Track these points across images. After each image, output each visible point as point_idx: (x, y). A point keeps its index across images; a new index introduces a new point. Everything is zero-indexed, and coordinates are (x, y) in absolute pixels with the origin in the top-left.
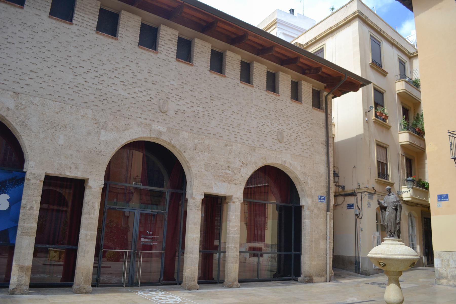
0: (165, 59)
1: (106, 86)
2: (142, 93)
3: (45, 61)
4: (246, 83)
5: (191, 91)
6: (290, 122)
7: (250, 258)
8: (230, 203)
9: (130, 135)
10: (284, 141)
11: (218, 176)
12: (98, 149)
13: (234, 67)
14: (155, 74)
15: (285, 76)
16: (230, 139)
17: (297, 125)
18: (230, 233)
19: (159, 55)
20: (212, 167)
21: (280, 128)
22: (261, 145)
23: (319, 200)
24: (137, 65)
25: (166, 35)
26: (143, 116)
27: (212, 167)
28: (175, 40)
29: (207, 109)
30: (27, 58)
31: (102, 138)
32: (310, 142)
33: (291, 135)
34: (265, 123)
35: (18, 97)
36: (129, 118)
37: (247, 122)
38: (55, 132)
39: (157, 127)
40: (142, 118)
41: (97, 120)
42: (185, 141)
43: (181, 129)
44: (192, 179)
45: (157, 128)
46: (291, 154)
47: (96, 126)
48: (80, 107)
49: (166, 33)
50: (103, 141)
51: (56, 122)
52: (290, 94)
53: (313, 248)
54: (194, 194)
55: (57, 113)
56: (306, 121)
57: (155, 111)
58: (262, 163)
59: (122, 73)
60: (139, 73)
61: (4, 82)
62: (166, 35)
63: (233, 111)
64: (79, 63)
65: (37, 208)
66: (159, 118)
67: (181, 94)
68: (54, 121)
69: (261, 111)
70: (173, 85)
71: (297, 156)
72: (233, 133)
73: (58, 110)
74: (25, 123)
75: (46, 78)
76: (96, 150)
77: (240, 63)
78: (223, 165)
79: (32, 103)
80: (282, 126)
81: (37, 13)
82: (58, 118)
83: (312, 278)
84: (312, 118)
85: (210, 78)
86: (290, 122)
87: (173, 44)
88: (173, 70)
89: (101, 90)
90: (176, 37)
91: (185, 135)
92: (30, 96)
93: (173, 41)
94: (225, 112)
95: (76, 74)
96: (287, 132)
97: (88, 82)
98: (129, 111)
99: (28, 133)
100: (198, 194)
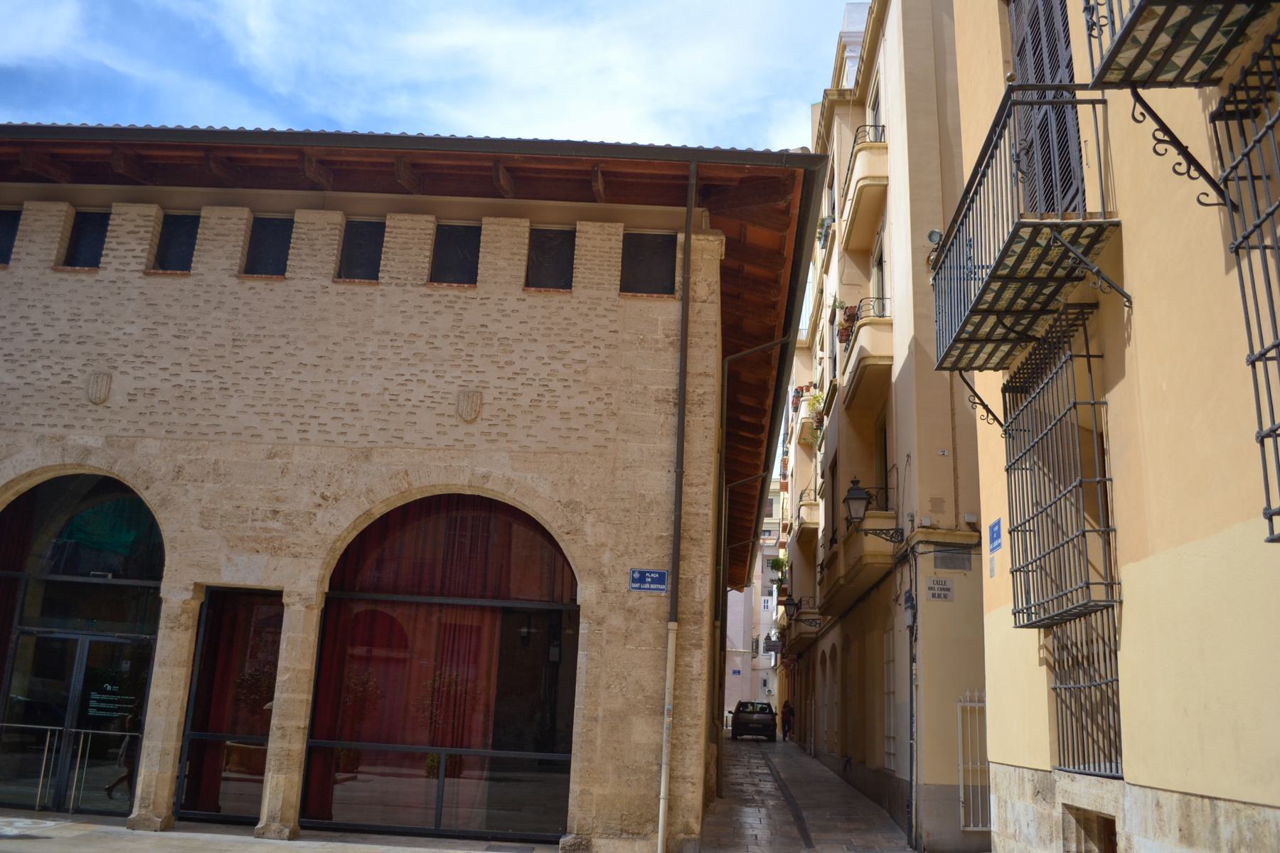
6: (514, 357)
11: (241, 539)
14: (86, 321)
17: (547, 360)
19: (101, 274)
20: (221, 516)
22: (392, 440)
23: (637, 585)
26: (48, 421)
27: (221, 516)
32: (600, 405)
33: (514, 394)
34: (412, 374)
43: (140, 434)
45: (81, 442)
49: (123, 220)
53: (599, 742)
56: (588, 343)
57: (78, 403)
67: (148, 353)
70: (130, 334)
71: (535, 454)
78: (257, 509)
83: (589, 841)
84: (614, 327)
86: (514, 357)
87: (141, 239)
91: (151, 446)
93: (139, 232)
94: (273, 371)
98: (19, 414)
100: (174, 588)
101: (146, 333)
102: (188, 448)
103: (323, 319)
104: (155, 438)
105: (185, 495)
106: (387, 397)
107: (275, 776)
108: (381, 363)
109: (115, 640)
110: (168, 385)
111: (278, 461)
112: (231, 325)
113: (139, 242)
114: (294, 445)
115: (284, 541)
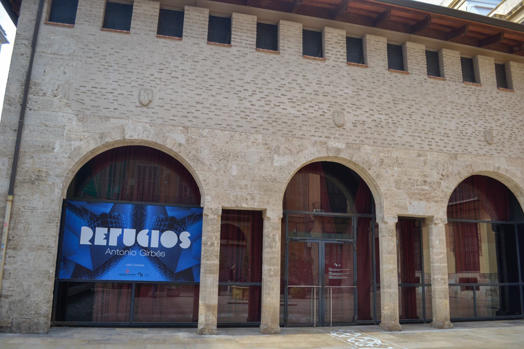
0: (334, 65)
1: (273, 106)
2: (313, 108)
3: (209, 90)
4: (435, 77)
5: (369, 97)
6: (500, 117)
7: (462, 292)
8: (431, 225)
9: (305, 157)
10: (495, 142)
11: (413, 194)
12: (273, 176)
13: (418, 60)
14: (325, 85)
15: (486, 59)
16: (423, 148)
17: (510, 120)
18: (435, 261)
19: (327, 62)
20: (404, 183)
21: (487, 126)
22: (464, 150)
24: (304, 77)
25: (332, 37)
26: (317, 134)
27: (404, 183)
28: (344, 42)
29: (390, 115)
30: (191, 90)
31: (276, 164)
33: (502, 133)
34: (466, 122)
35: (188, 131)
36: (302, 139)
37: (442, 124)
38: (227, 163)
39: (333, 144)
41: (268, 144)
42: (368, 157)
43: (362, 143)
44: (382, 201)
45: (335, 145)
46: (506, 158)
47: (268, 151)
48: (249, 133)
49: (332, 36)
50: (277, 167)
51: (227, 152)
52: (496, 82)
54: (386, 217)
55: (227, 143)
58: (468, 173)
59: (289, 90)
60: (308, 87)
61: (173, 118)
62: (332, 37)
63: (423, 114)
64: (243, 86)
65: (218, 244)
66: (335, 134)
67: (357, 103)
68: (225, 152)
69: (459, 108)
70: (347, 93)
71: (514, 159)
72: (426, 139)
73: (228, 140)
74: (198, 158)
75: (213, 108)
76: (270, 177)
77: (425, 54)
79: (202, 135)
80: (490, 124)
81: (196, 42)
82: (229, 148)
85: (390, 78)
86: (500, 117)
87: (341, 46)
88: (345, 76)
89: (269, 111)
90: (344, 38)
91: (368, 149)
92: (199, 129)
93: (340, 43)
94: (413, 116)
95: (241, 99)
96: (497, 130)
97: (255, 105)
99: (201, 167)
100: (390, 217)
101: (354, 93)
102: (384, 151)
103: (427, 94)
104: (368, 145)
105: (387, 173)
106: (459, 132)
107: (444, 300)
108: (454, 116)
109: (337, 242)
110: (369, 120)
111: (422, 158)
112: (391, 93)
113: (342, 48)
114: (427, 151)
115: (431, 195)
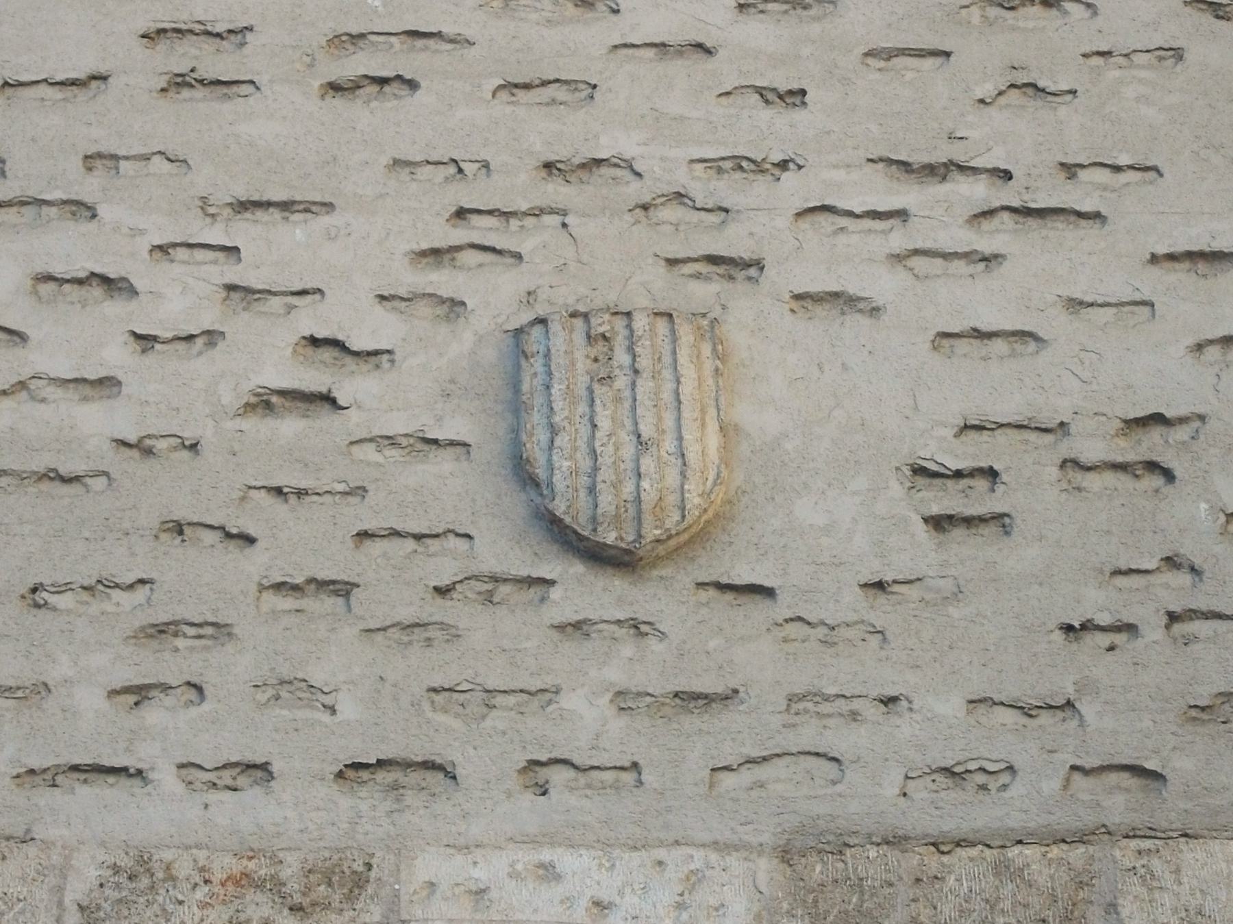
2: (115, 308)
40: (167, 778)
